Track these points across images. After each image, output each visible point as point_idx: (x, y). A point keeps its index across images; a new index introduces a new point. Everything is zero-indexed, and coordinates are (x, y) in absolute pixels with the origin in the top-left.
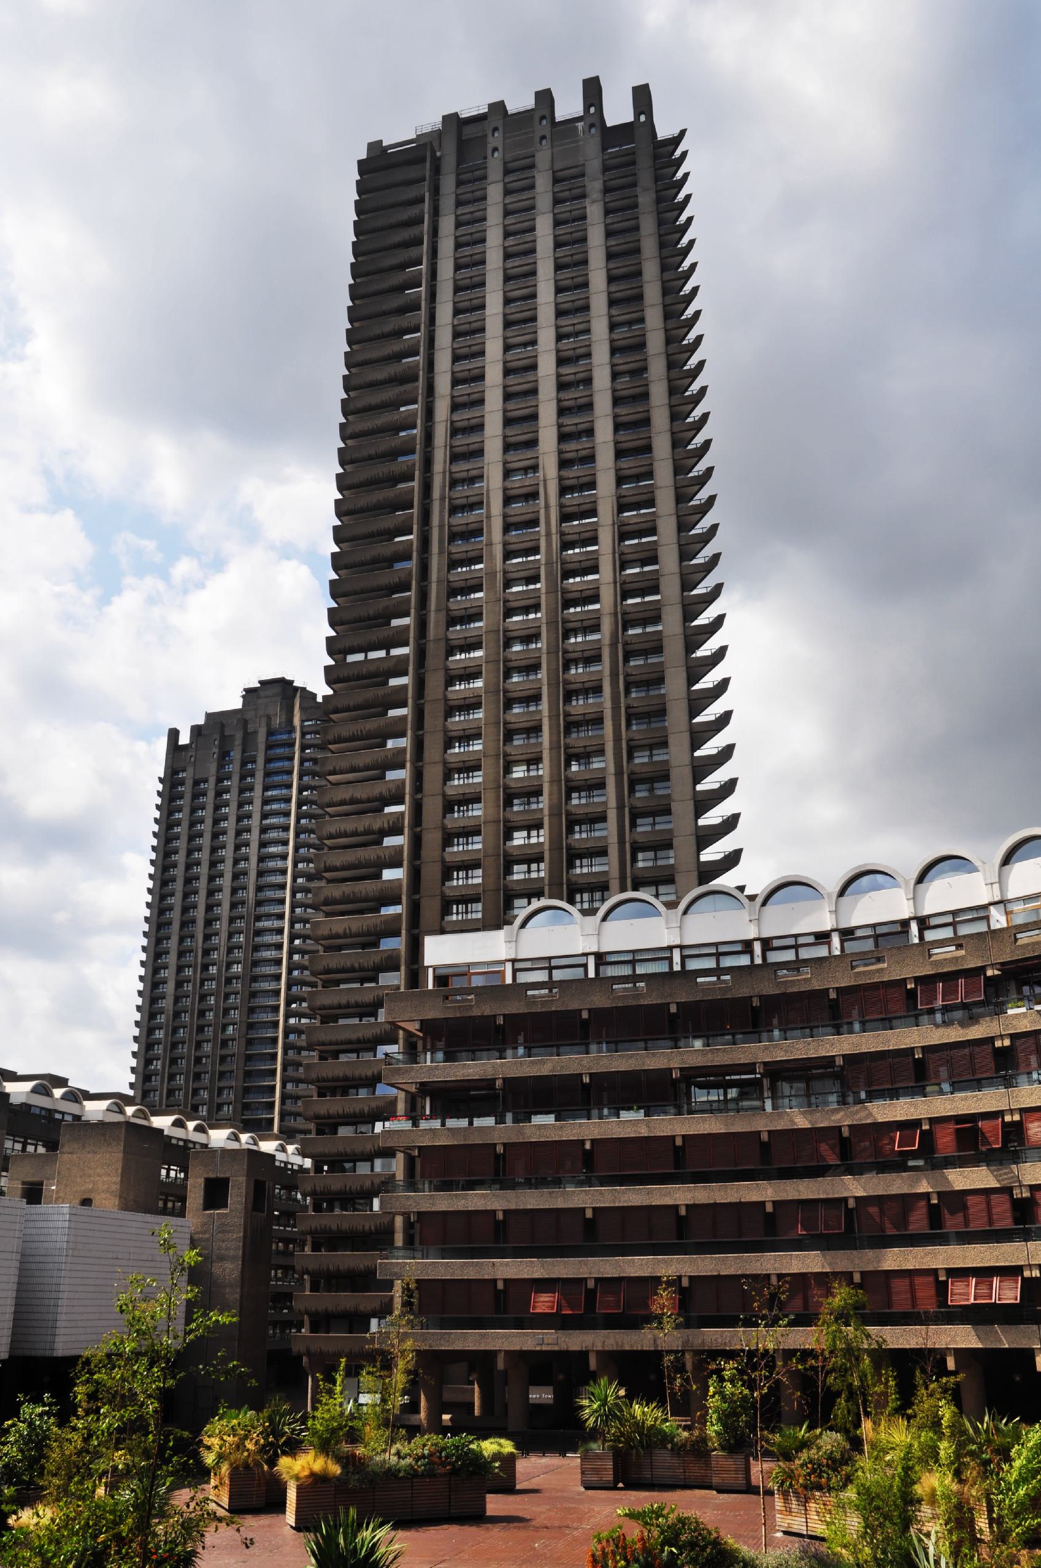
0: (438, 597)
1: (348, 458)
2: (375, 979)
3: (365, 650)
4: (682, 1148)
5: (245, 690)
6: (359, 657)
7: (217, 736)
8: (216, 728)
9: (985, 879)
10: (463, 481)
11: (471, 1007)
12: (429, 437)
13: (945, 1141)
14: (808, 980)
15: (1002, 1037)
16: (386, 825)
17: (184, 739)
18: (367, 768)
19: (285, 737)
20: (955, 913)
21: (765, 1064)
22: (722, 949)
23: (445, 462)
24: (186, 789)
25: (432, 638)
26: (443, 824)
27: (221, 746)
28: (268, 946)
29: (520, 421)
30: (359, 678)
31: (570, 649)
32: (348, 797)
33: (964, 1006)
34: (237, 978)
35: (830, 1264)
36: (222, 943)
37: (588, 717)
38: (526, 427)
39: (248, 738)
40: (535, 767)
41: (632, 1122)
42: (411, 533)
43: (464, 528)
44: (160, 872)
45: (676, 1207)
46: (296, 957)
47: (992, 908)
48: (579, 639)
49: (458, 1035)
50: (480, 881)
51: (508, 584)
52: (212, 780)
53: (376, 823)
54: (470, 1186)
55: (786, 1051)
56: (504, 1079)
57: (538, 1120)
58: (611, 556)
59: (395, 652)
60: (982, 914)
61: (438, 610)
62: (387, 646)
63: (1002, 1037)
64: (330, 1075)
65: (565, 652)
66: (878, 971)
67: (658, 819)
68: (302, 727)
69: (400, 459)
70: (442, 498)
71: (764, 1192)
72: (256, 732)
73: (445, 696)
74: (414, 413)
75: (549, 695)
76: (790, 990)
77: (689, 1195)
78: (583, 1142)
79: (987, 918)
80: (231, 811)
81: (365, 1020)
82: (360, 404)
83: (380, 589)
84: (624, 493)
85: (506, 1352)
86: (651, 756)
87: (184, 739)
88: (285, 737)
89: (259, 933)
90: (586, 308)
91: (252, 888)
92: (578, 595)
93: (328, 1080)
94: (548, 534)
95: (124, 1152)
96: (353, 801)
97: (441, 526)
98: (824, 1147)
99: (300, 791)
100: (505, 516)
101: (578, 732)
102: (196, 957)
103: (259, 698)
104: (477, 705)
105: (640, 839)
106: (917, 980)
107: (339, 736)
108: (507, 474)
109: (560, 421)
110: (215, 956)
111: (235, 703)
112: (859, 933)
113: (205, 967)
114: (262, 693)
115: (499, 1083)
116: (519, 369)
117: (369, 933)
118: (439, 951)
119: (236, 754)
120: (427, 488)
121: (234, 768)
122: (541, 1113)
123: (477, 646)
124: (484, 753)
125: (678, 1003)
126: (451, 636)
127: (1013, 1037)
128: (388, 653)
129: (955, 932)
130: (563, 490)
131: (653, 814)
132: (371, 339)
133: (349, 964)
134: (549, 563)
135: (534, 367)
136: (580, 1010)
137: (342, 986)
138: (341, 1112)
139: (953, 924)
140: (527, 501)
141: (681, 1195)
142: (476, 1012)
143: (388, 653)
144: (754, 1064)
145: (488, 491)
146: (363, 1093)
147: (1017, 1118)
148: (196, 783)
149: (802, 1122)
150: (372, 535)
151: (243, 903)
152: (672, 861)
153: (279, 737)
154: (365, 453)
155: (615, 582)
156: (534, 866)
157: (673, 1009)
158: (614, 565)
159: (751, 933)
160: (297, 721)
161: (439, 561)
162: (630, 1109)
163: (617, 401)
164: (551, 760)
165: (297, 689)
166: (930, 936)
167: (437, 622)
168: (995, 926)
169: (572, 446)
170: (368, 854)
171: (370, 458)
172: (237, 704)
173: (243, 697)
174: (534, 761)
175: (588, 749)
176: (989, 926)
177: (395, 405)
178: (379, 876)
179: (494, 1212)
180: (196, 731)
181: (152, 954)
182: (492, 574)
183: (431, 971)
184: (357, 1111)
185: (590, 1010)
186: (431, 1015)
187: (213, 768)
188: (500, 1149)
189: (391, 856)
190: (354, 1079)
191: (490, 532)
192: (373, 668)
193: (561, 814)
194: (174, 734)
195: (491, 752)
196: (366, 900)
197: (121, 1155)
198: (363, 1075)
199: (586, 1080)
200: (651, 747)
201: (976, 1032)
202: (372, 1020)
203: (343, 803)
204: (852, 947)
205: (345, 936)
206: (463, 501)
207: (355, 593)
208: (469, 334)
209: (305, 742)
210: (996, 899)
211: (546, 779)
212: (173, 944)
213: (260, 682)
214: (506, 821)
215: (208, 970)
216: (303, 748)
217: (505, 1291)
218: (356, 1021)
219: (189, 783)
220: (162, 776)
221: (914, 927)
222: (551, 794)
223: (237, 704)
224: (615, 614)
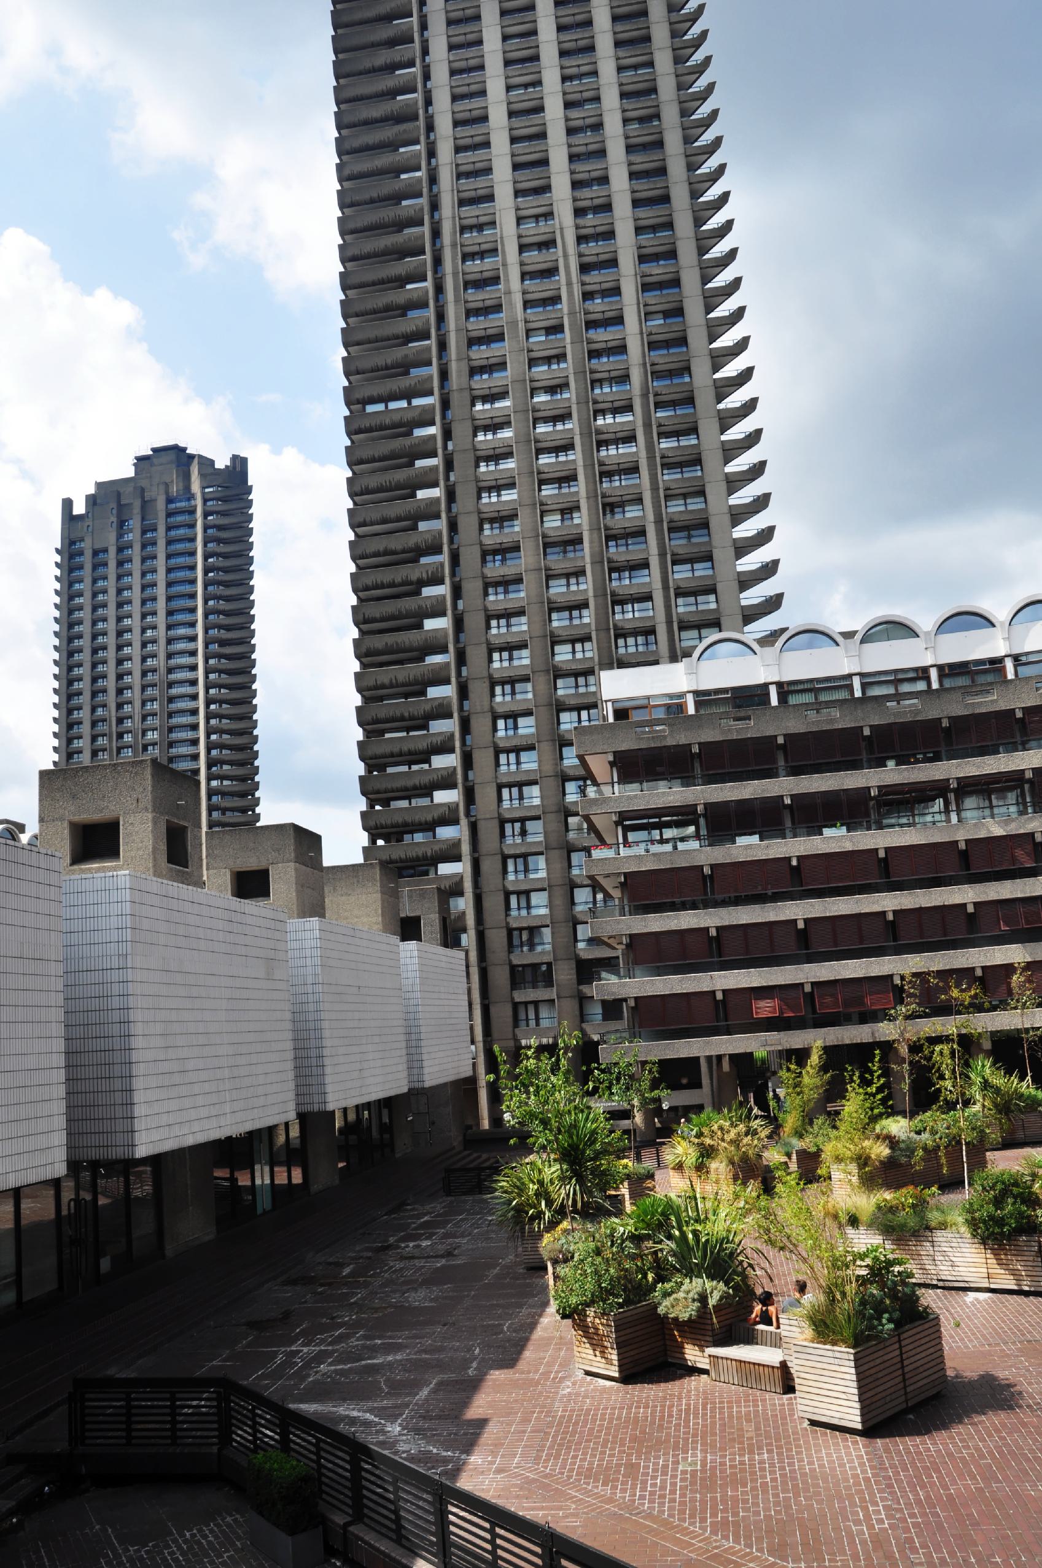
0: (457, 347)
1: (348, 200)
2: (425, 727)
3: (385, 399)
4: (797, 869)
5: (136, 458)
6: (380, 407)
7: (114, 505)
8: (107, 496)
10: (471, 228)
11: (665, 737)
12: (433, 179)
14: (910, 709)
16: (425, 576)
17: (79, 508)
18: (399, 519)
19: (183, 504)
21: (957, 778)
22: (900, 676)
23: (453, 207)
24: (87, 560)
25: (455, 388)
26: (482, 573)
27: (119, 515)
28: (182, 712)
29: (531, 165)
30: (382, 428)
31: (600, 399)
32: (381, 549)
34: (154, 744)
35: (1031, 954)
36: (136, 711)
37: (622, 466)
38: (537, 171)
39: (146, 505)
40: (569, 516)
41: (835, 839)
42: (426, 280)
43: (478, 276)
44: (65, 643)
45: (884, 913)
46: (213, 722)
48: (607, 390)
49: (633, 766)
50: (525, 628)
51: (529, 333)
52: (112, 550)
53: (413, 573)
54: (673, 907)
55: (978, 767)
56: (705, 804)
57: (742, 841)
58: (635, 307)
59: (416, 402)
61: (459, 360)
62: (408, 395)
64: (389, 822)
65: (595, 402)
67: (696, 566)
68: (203, 494)
69: (404, 203)
70: (454, 245)
71: (966, 895)
72: (154, 500)
73: (474, 446)
74: (418, 155)
75: (582, 445)
76: (977, 711)
77: (896, 902)
78: (789, 859)
80: (136, 581)
81: (415, 768)
82: (356, 143)
83: (396, 337)
84: (644, 243)
85: (731, 1056)
86: (686, 504)
87: (79, 508)
88: (183, 504)
89: (171, 700)
90: (591, 48)
91: (162, 656)
92: (603, 345)
93: (386, 827)
94: (569, 284)
95: (382, 893)
96: (386, 553)
97: (455, 274)
98: (1019, 853)
99: (206, 558)
100: (522, 264)
101: (611, 481)
102: (110, 726)
103: (152, 465)
104: (509, 455)
105: (683, 585)
107: (367, 488)
108: (579, 212)
109: (573, 167)
110: (128, 724)
111: (128, 471)
113: (120, 736)
114: (155, 461)
115: (700, 809)
116: (526, 110)
117: (416, 682)
118: (616, 685)
119: (135, 523)
120: (436, 234)
121: (133, 536)
122: (745, 834)
123: (503, 395)
124: (520, 502)
125: (871, 726)
126: (474, 386)
128: (409, 403)
130: (581, 239)
131: (568, 576)
132: (360, 73)
133: (398, 714)
134: (572, 313)
135: (540, 109)
136: (776, 736)
137: (387, 736)
138: (403, 856)
140: (540, 250)
141: (887, 902)
142: (670, 742)
143: (386, 407)
144: (948, 780)
145: (502, 238)
146: (419, 837)
148: (95, 553)
149: (998, 831)
150: (382, 282)
151: (154, 671)
152: (713, 606)
153: (179, 505)
154: (366, 196)
155: (641, 333)
156: (575, 613)
157: (867, 732)
158: (640, 316)
159: (928, 660)
160: (196, 487)
161: (456, 309)
162: (835, 826)
163: (630, 149)
164: (589, 509)
165: (192, 457)
167: (459, 371)
169: (586, 193)
170: (408, 604)
171: (372, 201)
172: (130, 472)
173: (135, 465)
174: (568, 511)
175: (625, 498)
177: (393, 146)
178: (420, 626)
179: (707, 929)
180: (91, 500)
181: (65, 725)
182: (514, 323)
183: (610, 704)
184: (420, 854)
185: (785, 736)
186: (624, 747)
187: (112, 537)
188: (707, 871)
189: (432, 606)
190: (413, 824)
191: (507, 280)
192: (396, 418)
193: (602, 562)
194: (68, 504)
195: (528, 501)
196: (411, 650)
197: (379, 895)
198: (423, 820)
199: (788, 801)
200: (685, 496)
202: (426, 766)
203: (377, 554)
204: (1024, 671)
205: (391, 686)
206: (476, 248)
207: (369, 342)
208: (468, 69)
209: (208, 509)
211: (586, 527)
212: (84, 715)
213: (154, 450)
214: (547, 569)
215: (122, 738)
216: (206, 515)
217: (724, 1001)
218: (405, 768)
219: (88, 553)
220: (59, 547)
222: (591, 542)
223: (130, 472)
224: (644, 364)
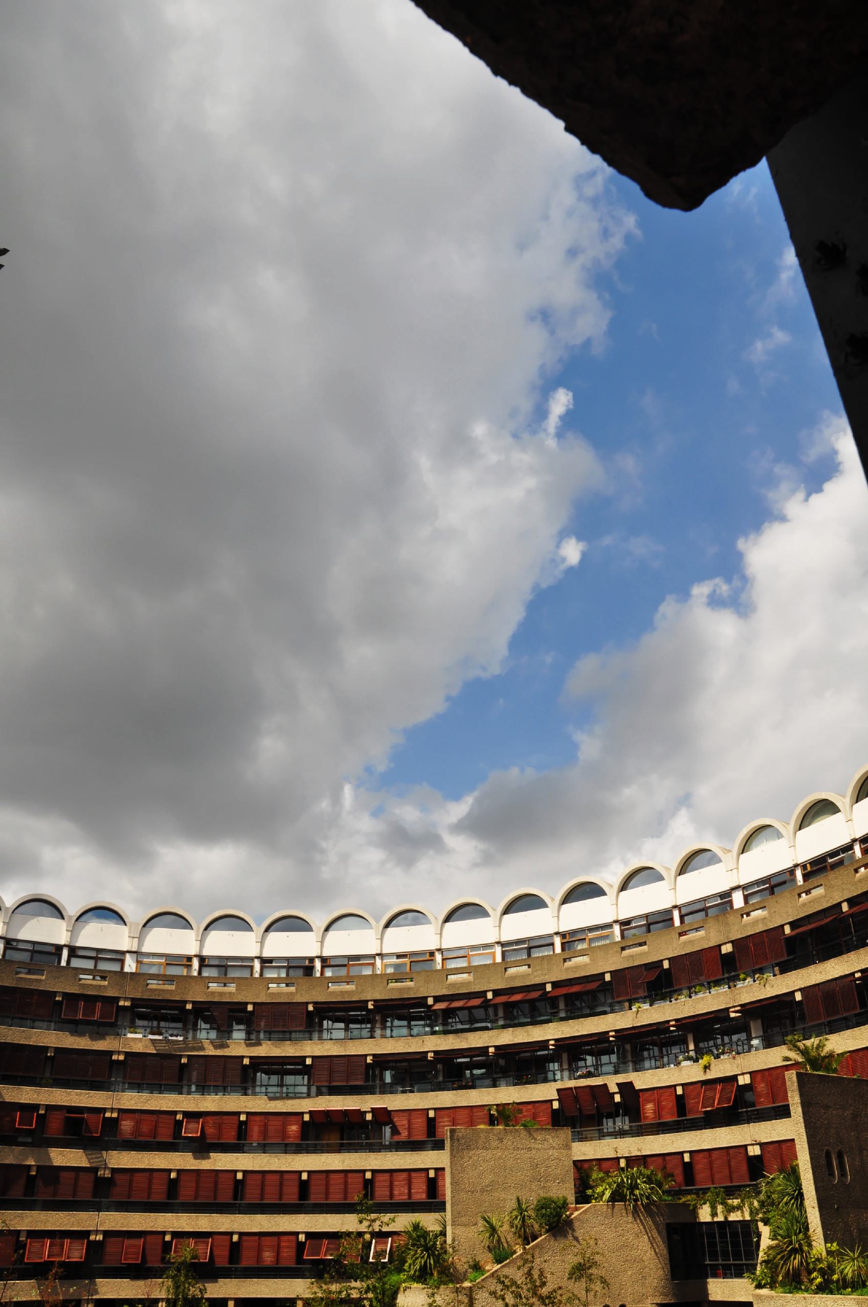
9: (130, 933)
13: (55, 1125)
15: (119, 1053)
20: (99, 951)
33: (98, 1024)
47: (128, 955)
60: (118, 957)
63: (119, 1053)
66: (36, 980)
79: (122, 962)
106: (65, 995)
112: (21, 946)
127: (127, 1054)
129: (96, 966)
139: (96, 959)
147: (115, 1115)
166: (76, 963)
168: (127, 969)
176: (122, 968)
201: (101, 1045)
210: (134, 949)
221: (65, 953)
